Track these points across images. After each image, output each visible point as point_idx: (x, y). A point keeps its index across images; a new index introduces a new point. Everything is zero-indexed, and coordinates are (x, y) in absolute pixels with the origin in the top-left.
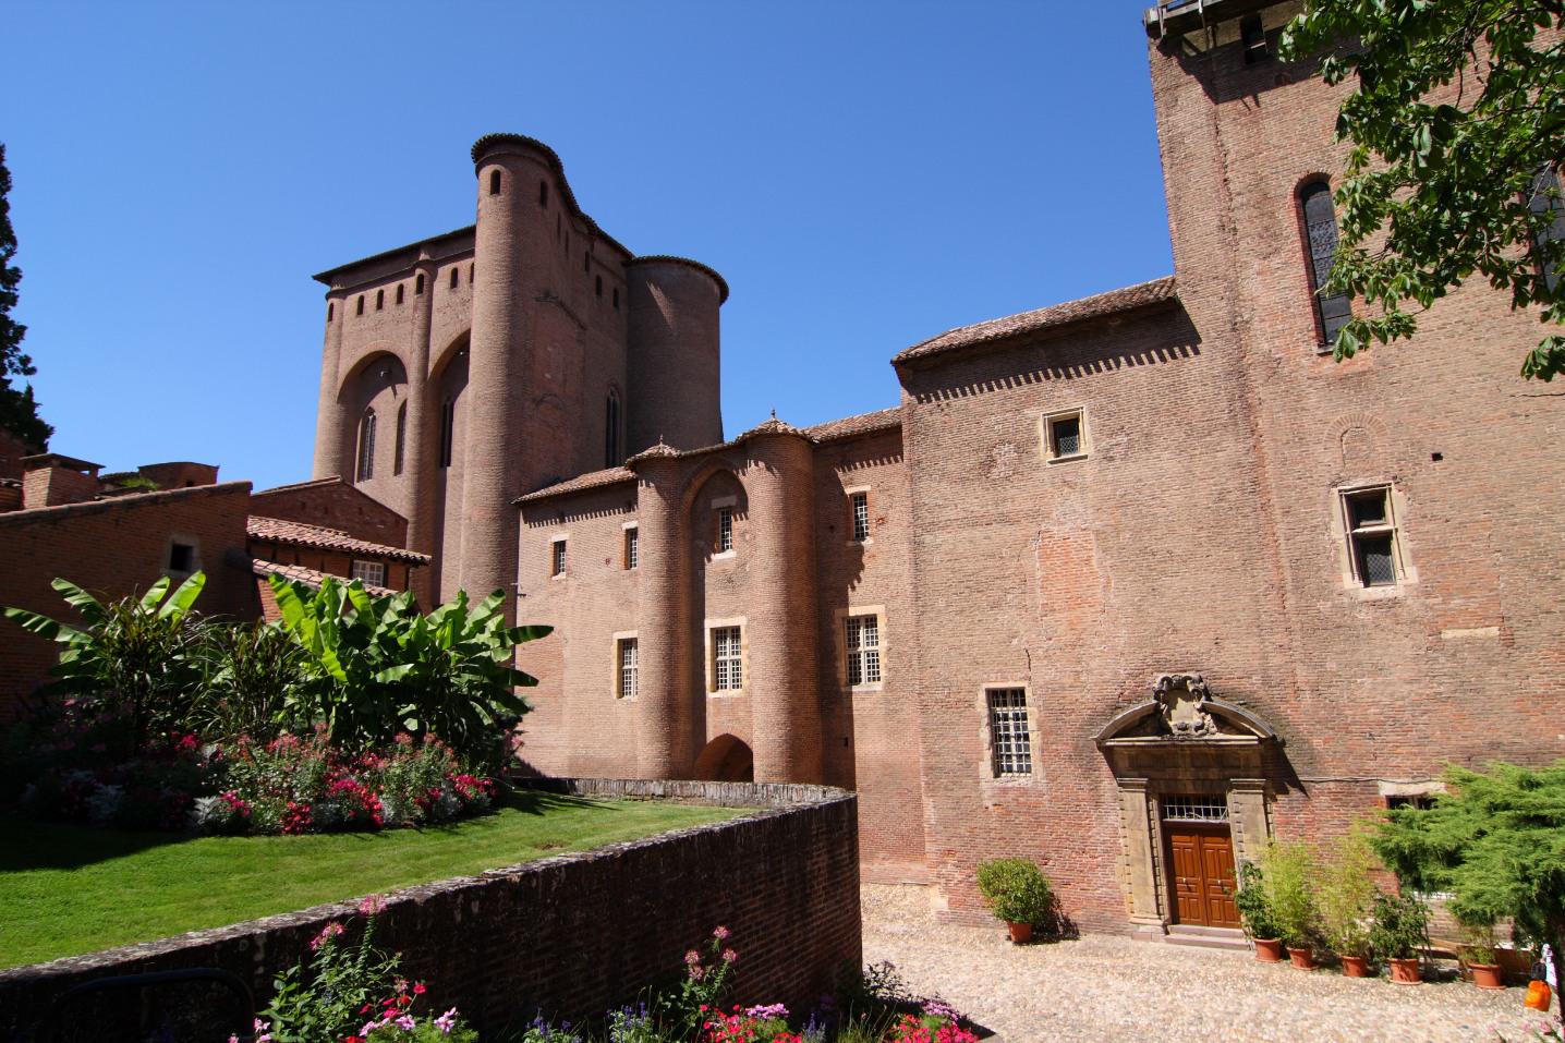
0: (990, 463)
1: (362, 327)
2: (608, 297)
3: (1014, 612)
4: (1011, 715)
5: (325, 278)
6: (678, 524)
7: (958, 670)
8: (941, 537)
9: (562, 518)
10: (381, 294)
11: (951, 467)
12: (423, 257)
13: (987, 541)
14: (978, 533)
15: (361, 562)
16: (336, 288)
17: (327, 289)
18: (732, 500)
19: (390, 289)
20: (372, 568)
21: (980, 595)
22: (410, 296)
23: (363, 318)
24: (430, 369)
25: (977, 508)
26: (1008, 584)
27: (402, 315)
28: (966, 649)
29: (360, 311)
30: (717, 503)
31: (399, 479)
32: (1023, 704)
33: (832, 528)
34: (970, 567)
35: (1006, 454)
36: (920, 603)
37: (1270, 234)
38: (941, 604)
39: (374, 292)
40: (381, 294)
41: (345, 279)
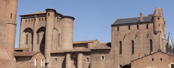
0: (97, 59)
2: (59, 22)
9: (56, 56)
18: (75, 57)
19: (30, 19)
24: (36, 31)
30: (74, 57)
35: (98, 58)
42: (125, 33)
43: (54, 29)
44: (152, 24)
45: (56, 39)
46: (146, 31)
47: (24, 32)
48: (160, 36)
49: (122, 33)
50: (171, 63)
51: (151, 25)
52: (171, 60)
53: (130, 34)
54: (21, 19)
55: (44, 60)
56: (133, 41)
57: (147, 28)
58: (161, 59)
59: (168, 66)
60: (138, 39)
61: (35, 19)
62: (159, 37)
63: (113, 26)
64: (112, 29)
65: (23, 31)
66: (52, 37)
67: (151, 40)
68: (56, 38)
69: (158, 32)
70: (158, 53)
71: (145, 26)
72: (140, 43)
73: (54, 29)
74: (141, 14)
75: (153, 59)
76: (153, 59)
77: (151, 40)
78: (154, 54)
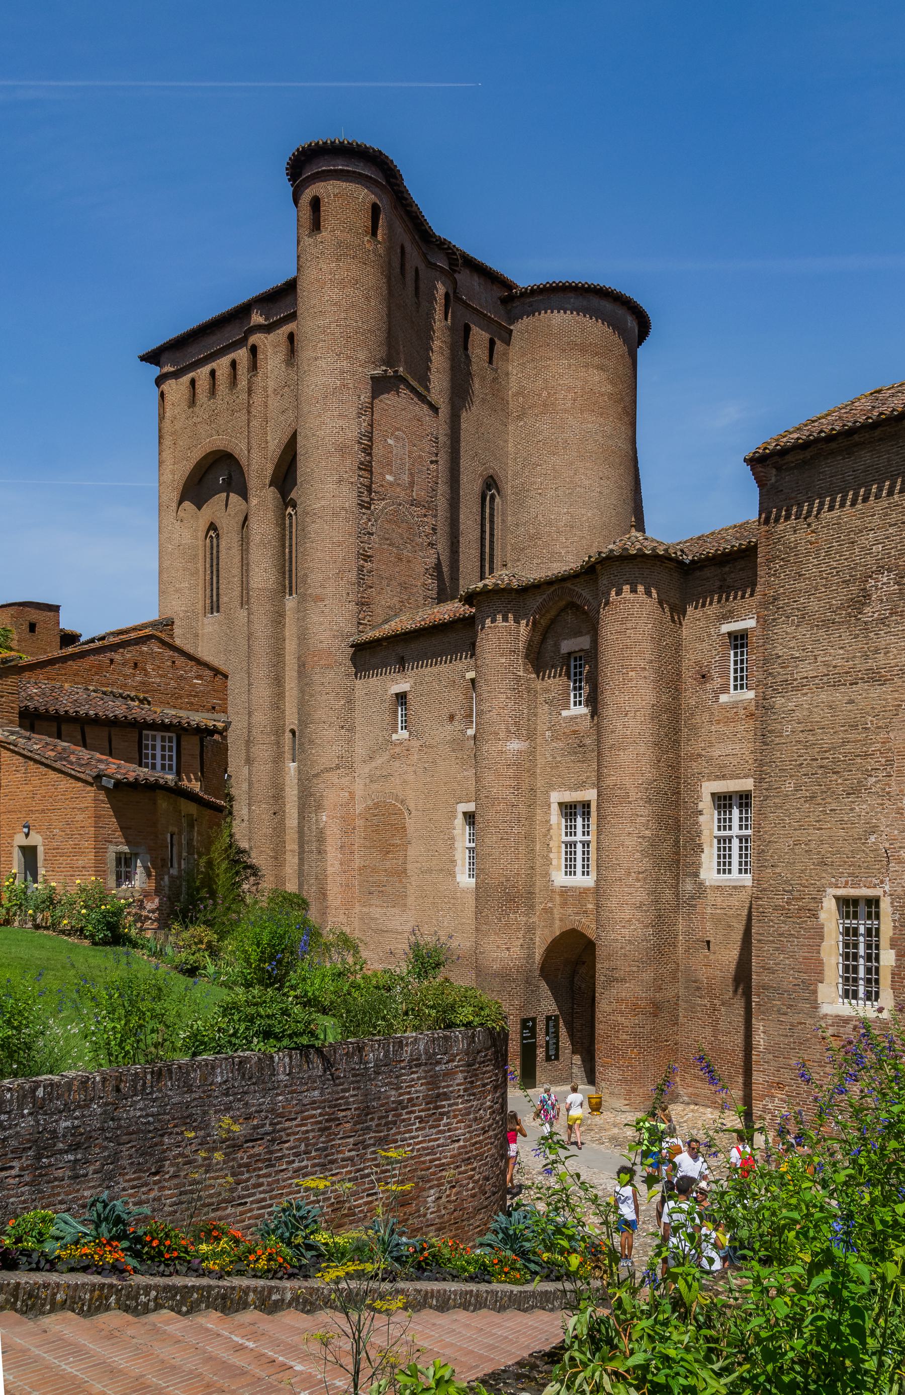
1: (195, 419)
3: (874, 801)
4: (862, 930)
5: (152, 357)
6: (521, 673)
7: (803, 871)
8: (798, 699)
9: (402, 663)
10: (213, 373)
11: (814, 605)
13: (850, 707)
14: (839, 696)
15: (150, 733)
16: (168, 369)
17: (156, 371)
18: (583, 642)
20: (163, 739)
21: (835, 777)
22: (243, 383)
23: (196, 409)
25: (839, 662)
26: (871, 764)
27: (237, 401)
28: (813, 845)
29: (192, 401)
30: (566, 646)
32: (878, 917)
33: (703, 677)
34: (827, 740)
36: (765, 786)
38: (789, 786)
40: (213, 373)
41: (175, 355)
47: (187, 504)
65: (175, 496)
66: (366, 467)
68: (419, 493)
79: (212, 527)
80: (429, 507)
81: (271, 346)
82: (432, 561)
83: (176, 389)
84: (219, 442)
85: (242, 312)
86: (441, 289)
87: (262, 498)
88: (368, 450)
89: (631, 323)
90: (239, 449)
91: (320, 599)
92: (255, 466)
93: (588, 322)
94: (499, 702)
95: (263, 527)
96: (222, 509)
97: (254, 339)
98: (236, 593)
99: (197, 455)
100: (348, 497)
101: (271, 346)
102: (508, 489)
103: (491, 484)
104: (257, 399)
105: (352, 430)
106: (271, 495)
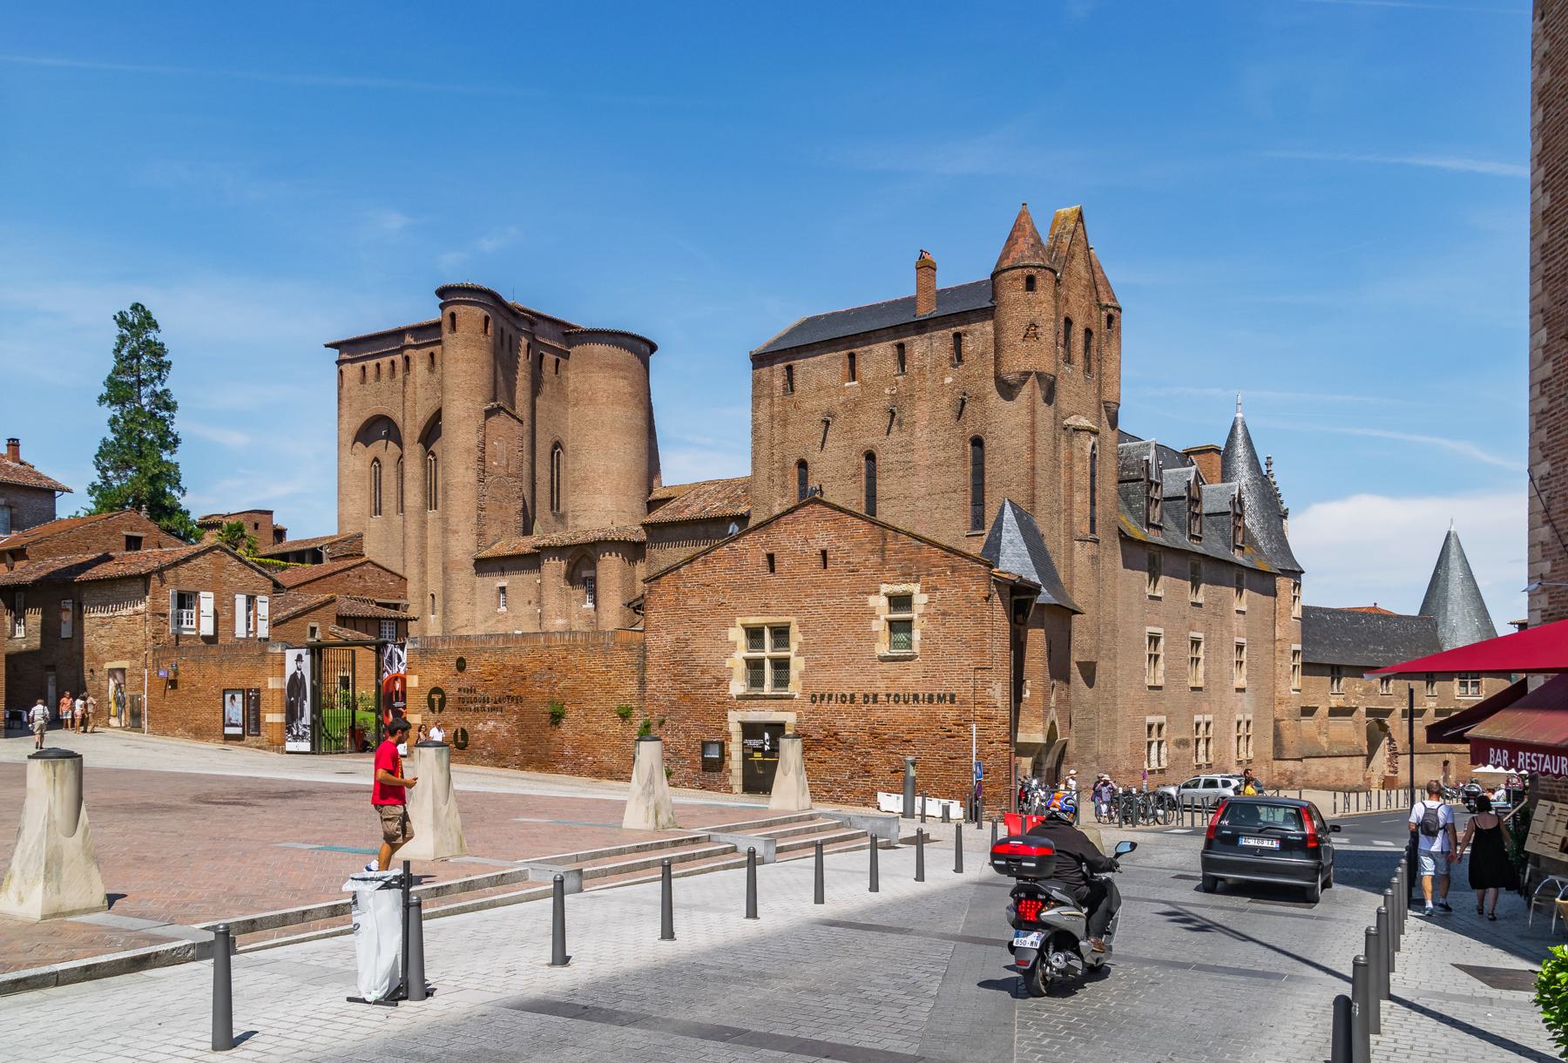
12: (409, 340)
19: (385, 362)
22: (399, 375)
24: (418, 434)
30: (585, 574)
31: (398, 519)
37: (784, 486)
39: (373, 362)
40: (378, 365)
41: (352, 349)
42: (825, 403)
43: (489, 414)
44: (988, 327)
45: (509, 475)
46: (948, 380)
47: (358, 444)
48: (1033, 412)
49: (807, 405)
50: (885, 588)
51: (979, 336)
52: (884, 561)
53: (854, 406)
54: (339, 363)
55: (259, 598)
56: (870, 456)
57: (958, 356)
58: (824, 553)
59: (865, 604)
60: (905, 437)
61: (407, 359)
62: (1028, 420)
63: (761, 360)
64: (757, 382)
65: (351, 438)
66: (482, 460)
67: (977, 442)
68: (512, 469)
69: (1024, 382)
70: (802, 512)
71: (940, 341)
72: (909, 468)
73: (489, 414)
74: (925, 266)
75: (771, 557)
76: (771, 557)
77: (977, 442)
78: (783, 520)
79: (376, 460)
80: (518, 477)
81: (419, 358)
82: (520, 506)
83: (352, 370)
84: (384, 410)
85: (399, 334)
86: (524, 341)
87: (413, 451)
88: (483, 450)
89: (645, 348)
90: (397, 417)
91: (456, 532)
92: (408, 430)
93: (615, 350)
94: (552, 601)
95: (413, 467)
96: (384, 450)
97: (407, 352)
98: (394, 504)
99: (367, 415)
100: (472, 477)
101: (419, 358)
102: (568, 447)
103: (557, 445)
104: (409, 389)
105: (474, 440)
106: (418, 448)
